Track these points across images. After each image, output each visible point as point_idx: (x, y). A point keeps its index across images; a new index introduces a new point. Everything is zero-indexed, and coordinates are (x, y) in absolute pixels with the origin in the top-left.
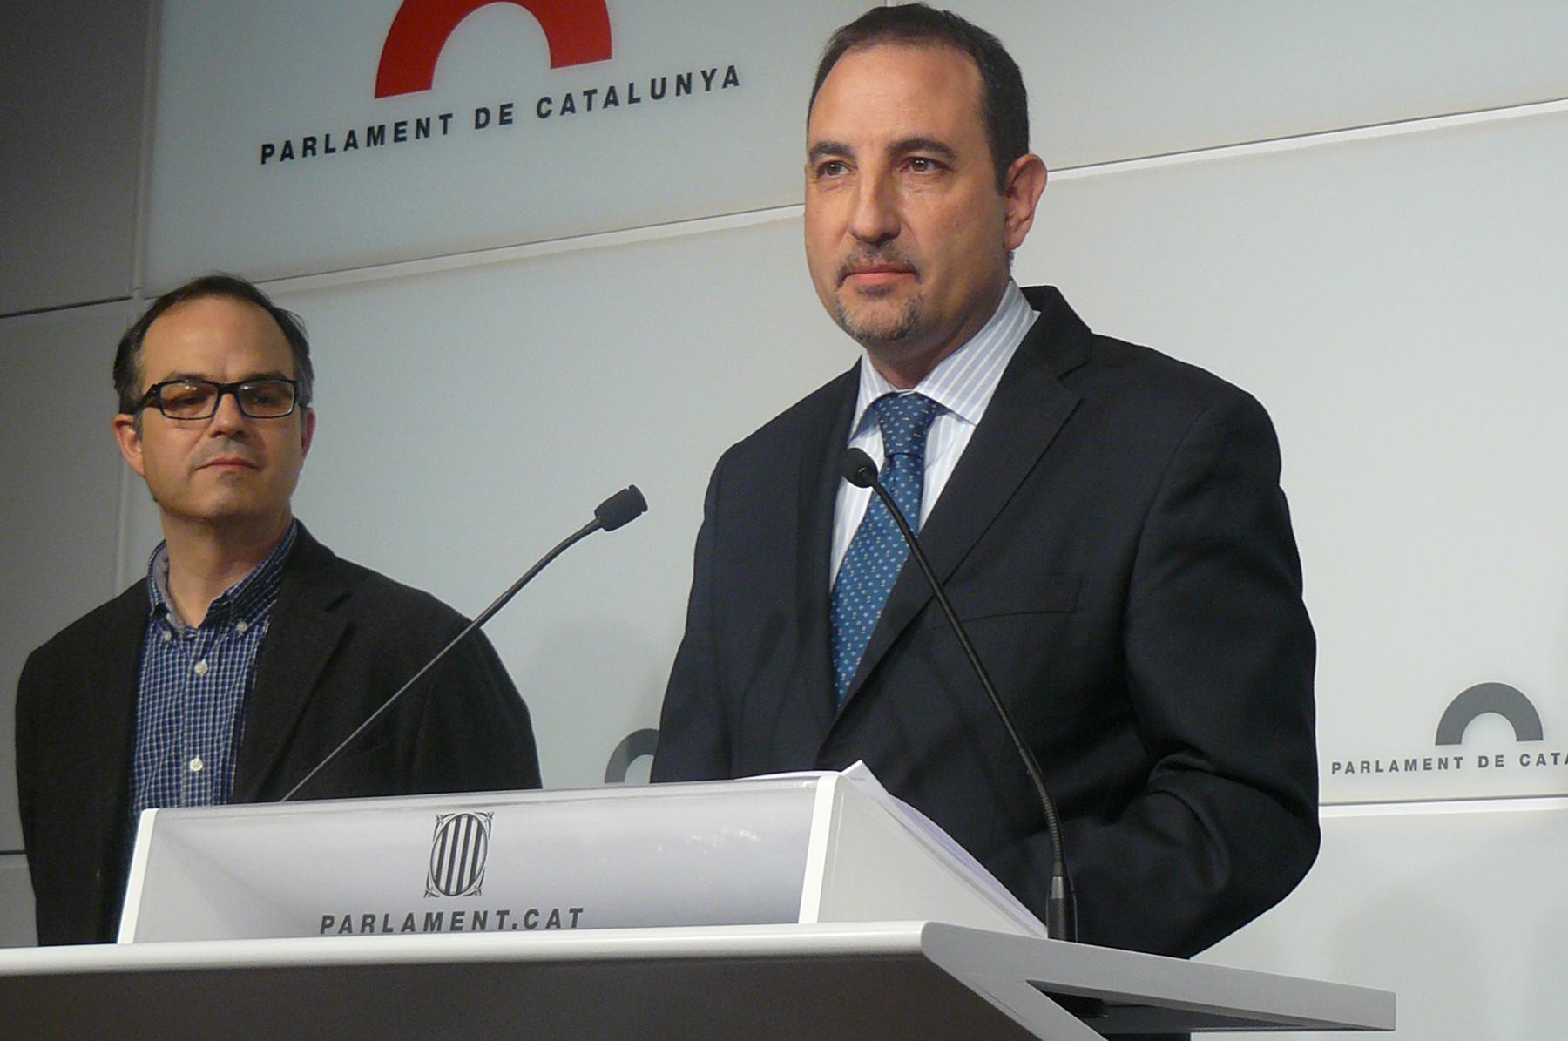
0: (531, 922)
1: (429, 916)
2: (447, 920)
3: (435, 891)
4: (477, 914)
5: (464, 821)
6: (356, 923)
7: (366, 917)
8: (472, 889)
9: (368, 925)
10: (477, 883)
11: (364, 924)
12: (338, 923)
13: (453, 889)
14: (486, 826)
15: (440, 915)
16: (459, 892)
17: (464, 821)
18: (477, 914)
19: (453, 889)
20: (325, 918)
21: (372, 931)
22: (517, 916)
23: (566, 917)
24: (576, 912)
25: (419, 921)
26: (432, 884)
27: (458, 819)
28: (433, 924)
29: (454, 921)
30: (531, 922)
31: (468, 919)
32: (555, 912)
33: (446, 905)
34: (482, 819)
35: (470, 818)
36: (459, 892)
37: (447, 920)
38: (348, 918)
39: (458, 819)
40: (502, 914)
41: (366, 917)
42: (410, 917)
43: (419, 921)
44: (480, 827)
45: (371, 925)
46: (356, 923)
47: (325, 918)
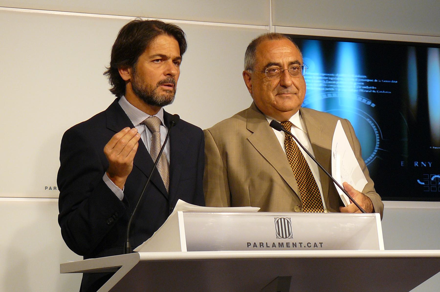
0: (309, 246)
1: (279, 243)
2: (285, 245)
3: (279, 237)
4: (293, 243)
5: (283, 220)
6: (258, 245)
7: (260, 243)
8: (290, 237)
9: (261, 246)
10: (291, 235)
11: (260, 245)
12: (252, 245)
13: (284, 237)
14: (289, 221)
15: (282, 243)
16: (286, 237)
17: (283, 220)
18: (293, 243)
19: (284, 237)
20: (248, 243)
21: (263, 247)
22: (304, 244)
23: (319, 245)
24: (321, 243)
25: (277, 245)
26: (278, 235)
27: (281, 219)
28: (281, 245)
29: (287, 245)
30: (309, 246)
31: (291, 245)
32: (315, 243)
33: (285, 241)
34: (288, 219)
35: (284, 219)
36: (286, 237)
37: (285, 245)
38: (255, 243)
39: (281, 219)
40: (301, 243)
41: (260, 243)
42: (274, 243)
43: (277, 245)
44: (288, 222)
45: (263, 245)
46: (258, 245)
47: (248, 243)
